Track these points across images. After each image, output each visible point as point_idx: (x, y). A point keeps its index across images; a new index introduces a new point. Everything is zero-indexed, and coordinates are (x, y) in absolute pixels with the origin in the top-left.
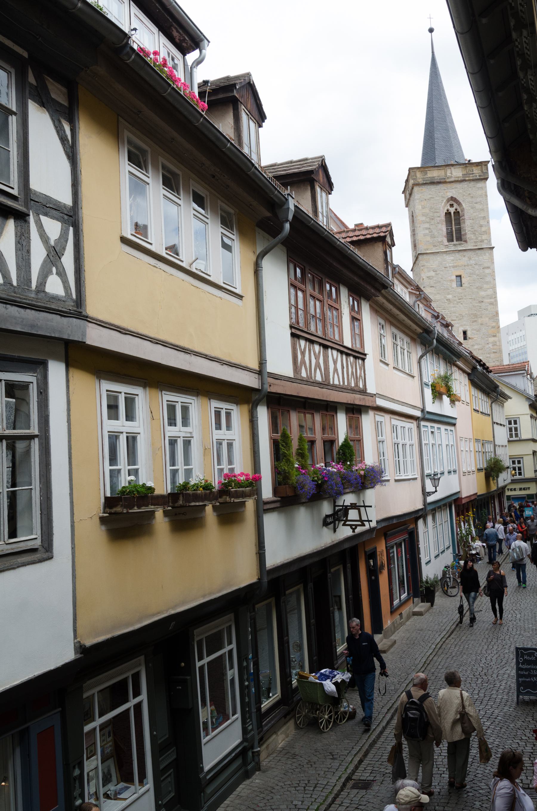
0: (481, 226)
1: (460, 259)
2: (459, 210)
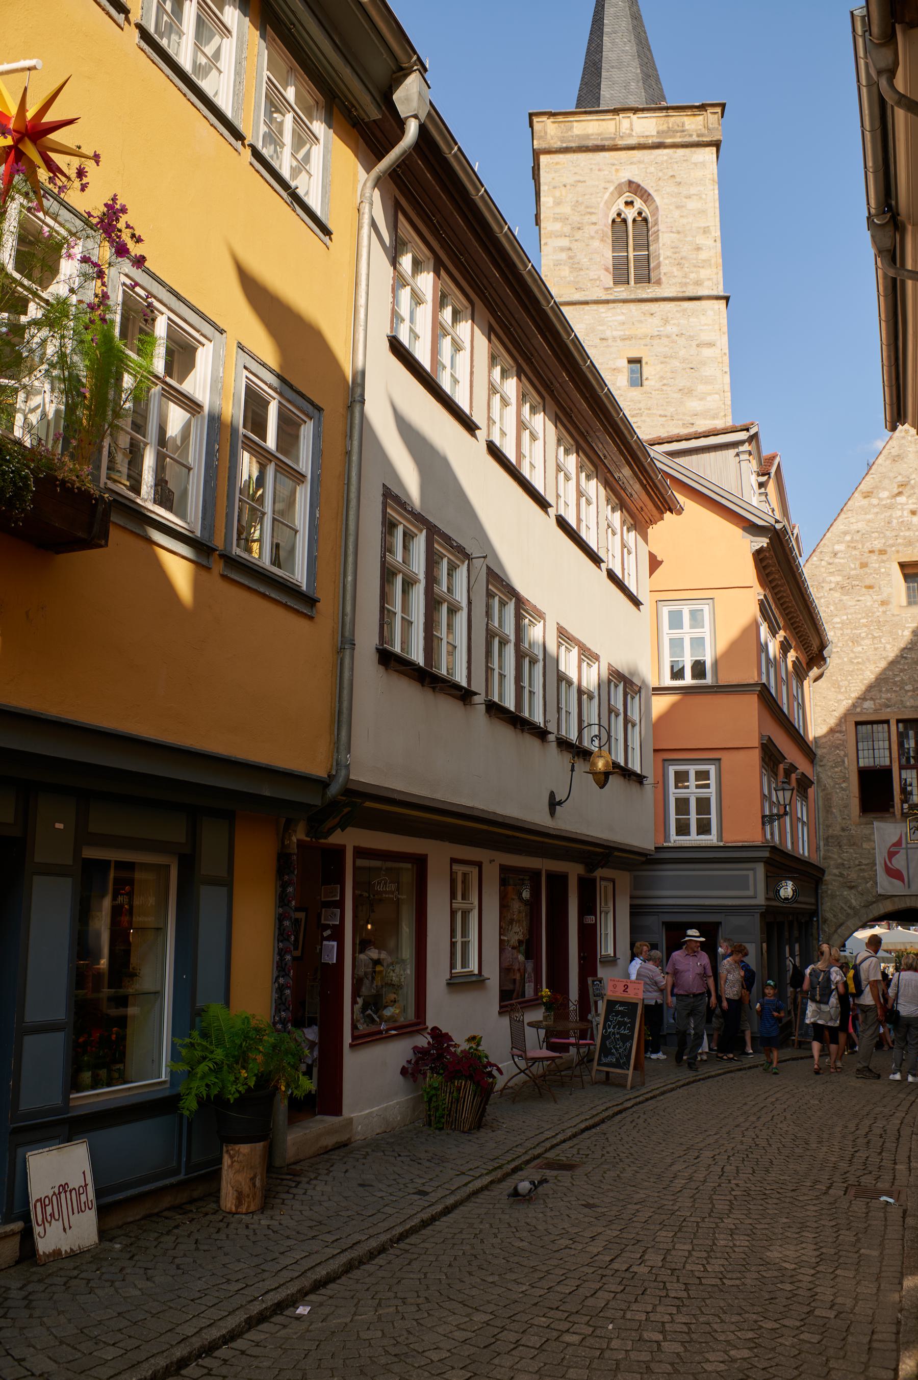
0: (698, 249)
1: (641, 322)
2: (647, 212)
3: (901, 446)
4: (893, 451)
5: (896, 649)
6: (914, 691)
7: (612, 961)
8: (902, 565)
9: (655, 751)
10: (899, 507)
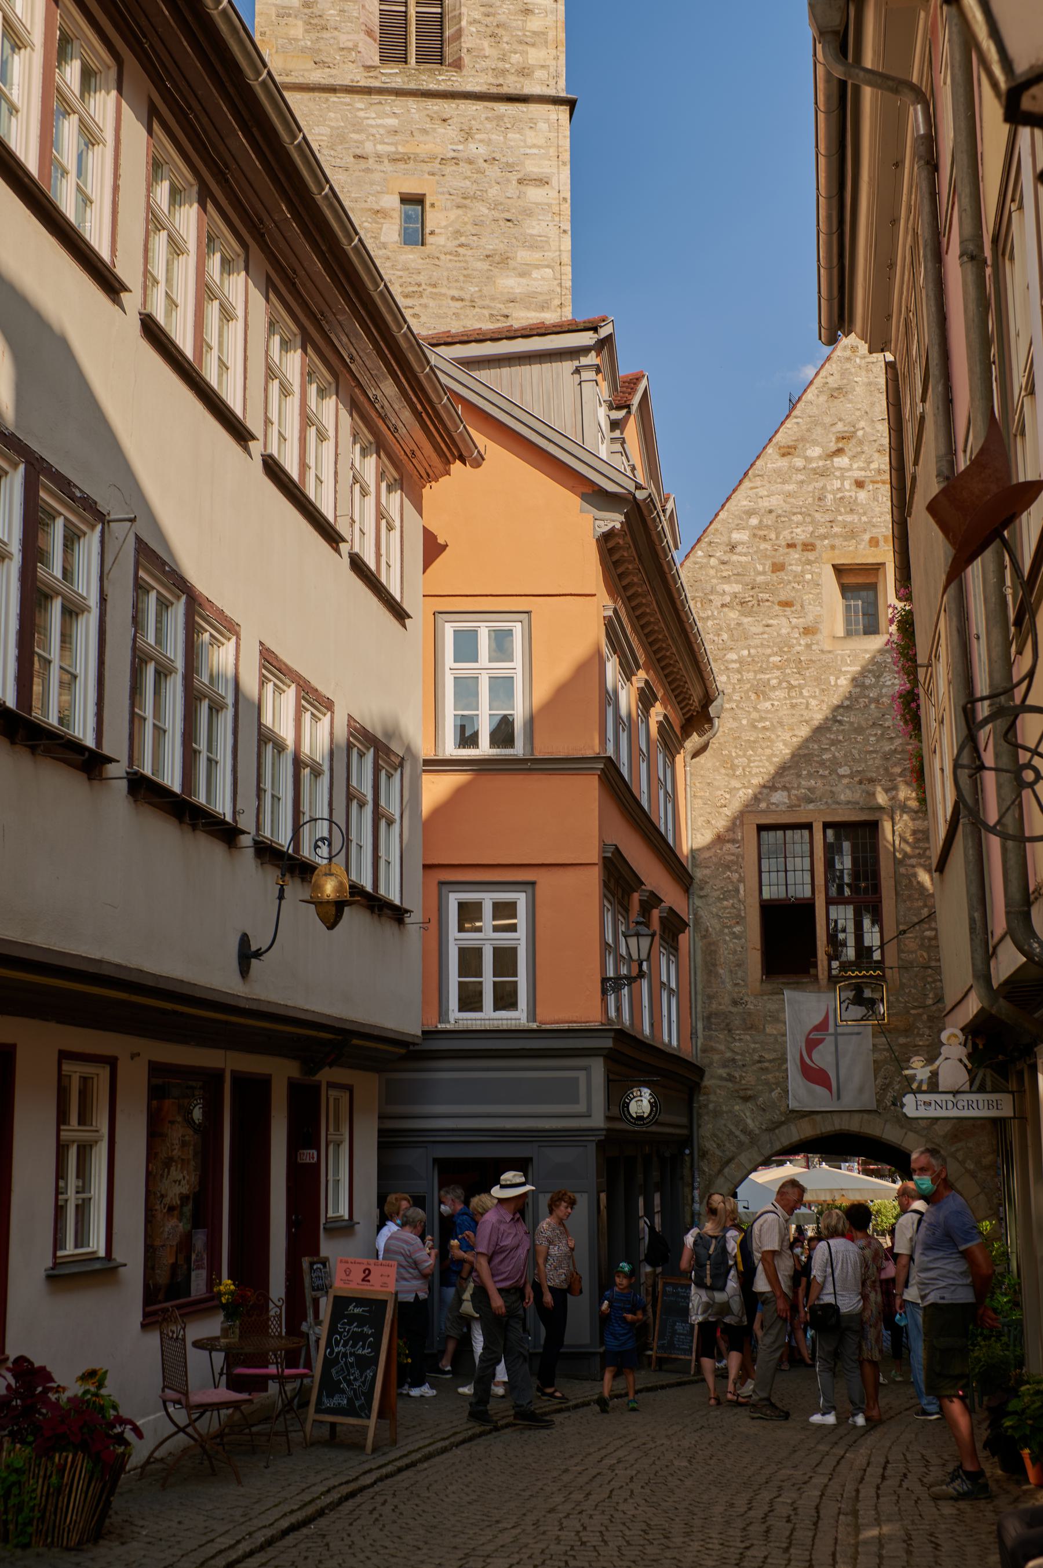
1: (424, 131)
3: (843, 373)
4: (830, 380)
5: (825, 707)
6: (851, 776)
7: (345, 1228)
8: (839, 570)
9: (426, 867)
10: (838, 474)
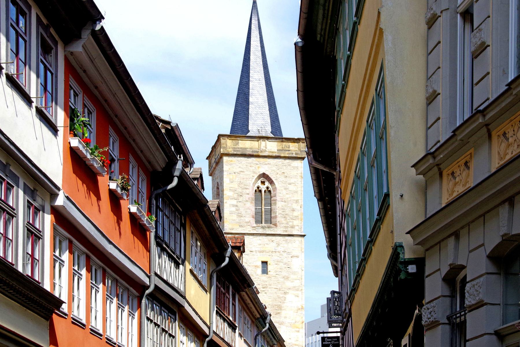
0: (293, 210)
1: (267, 244)
2: (271, 188)
